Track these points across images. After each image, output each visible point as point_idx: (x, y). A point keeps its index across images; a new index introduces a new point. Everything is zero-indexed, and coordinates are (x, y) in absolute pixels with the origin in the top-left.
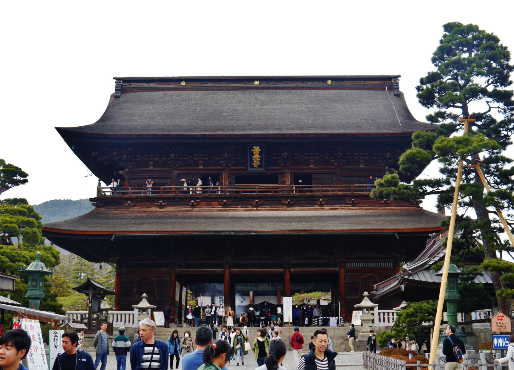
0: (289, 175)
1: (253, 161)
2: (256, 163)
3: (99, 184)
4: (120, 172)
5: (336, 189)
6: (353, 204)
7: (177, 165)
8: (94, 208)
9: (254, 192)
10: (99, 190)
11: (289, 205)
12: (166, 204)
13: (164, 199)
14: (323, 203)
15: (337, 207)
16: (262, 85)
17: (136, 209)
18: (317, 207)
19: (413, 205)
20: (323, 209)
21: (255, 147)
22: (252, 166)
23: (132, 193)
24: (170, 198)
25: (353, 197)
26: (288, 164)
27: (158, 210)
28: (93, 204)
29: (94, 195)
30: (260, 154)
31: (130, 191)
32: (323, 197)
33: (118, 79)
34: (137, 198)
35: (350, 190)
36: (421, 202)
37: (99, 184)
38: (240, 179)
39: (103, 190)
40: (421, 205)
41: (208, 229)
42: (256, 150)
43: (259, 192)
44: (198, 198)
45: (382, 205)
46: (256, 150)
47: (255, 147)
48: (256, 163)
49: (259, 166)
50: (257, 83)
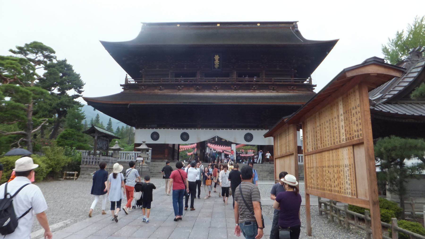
0: (235, 73)
1: (215, 65)
2: (217, 66)
3: (126, 77)
4: (140, 71)
5: (263, 80)
6: (273, 90)
7: (172, 67)
8: (123, 90)
9: (215, 81)
10: (126, 80)
11: (235, 89)
12: (163, 88)
13: (163, 85)
14: (256, 88)
15: (264, 91)
16: (221, 26)
17: (147, 92)
18: (252, 91)
19: (309, 90)
20: (255, 92)
21: (216, 56)
22: (214, 68)
23: (145, 82)
24: (166, 85)
25: (273, 85)
26: (235, 67)
27: (159, 91)
28: (123, 88)
29: (124, 83)
30: (219, 60)
31: (144, 80)
32: (256, 85)
33: (144, 23)
34: (147, 85)
35: (270, 81)
36: (314, 89)
37: (126, 77)
38: (207, 75)
39: (129, 80)
40: (314, 91)
41: (186, 101)
42: (217, 57)
43: (218, 81)
44: (182, 85)
45: (291, 90)
46: (217, 57)
47: (216, 56)
48: (217, 66)
49: (219, 68)
50: (218, 25)
